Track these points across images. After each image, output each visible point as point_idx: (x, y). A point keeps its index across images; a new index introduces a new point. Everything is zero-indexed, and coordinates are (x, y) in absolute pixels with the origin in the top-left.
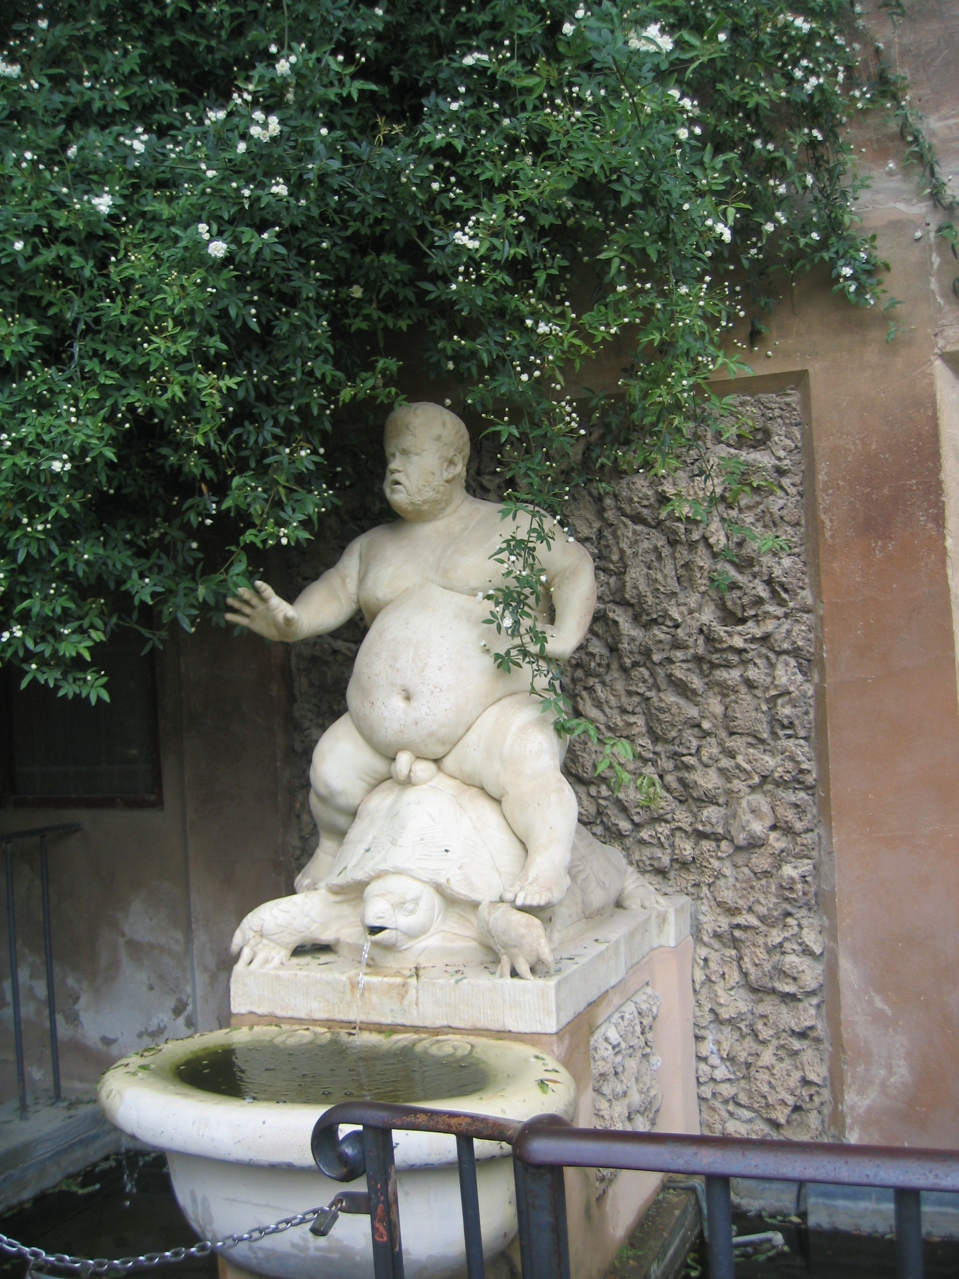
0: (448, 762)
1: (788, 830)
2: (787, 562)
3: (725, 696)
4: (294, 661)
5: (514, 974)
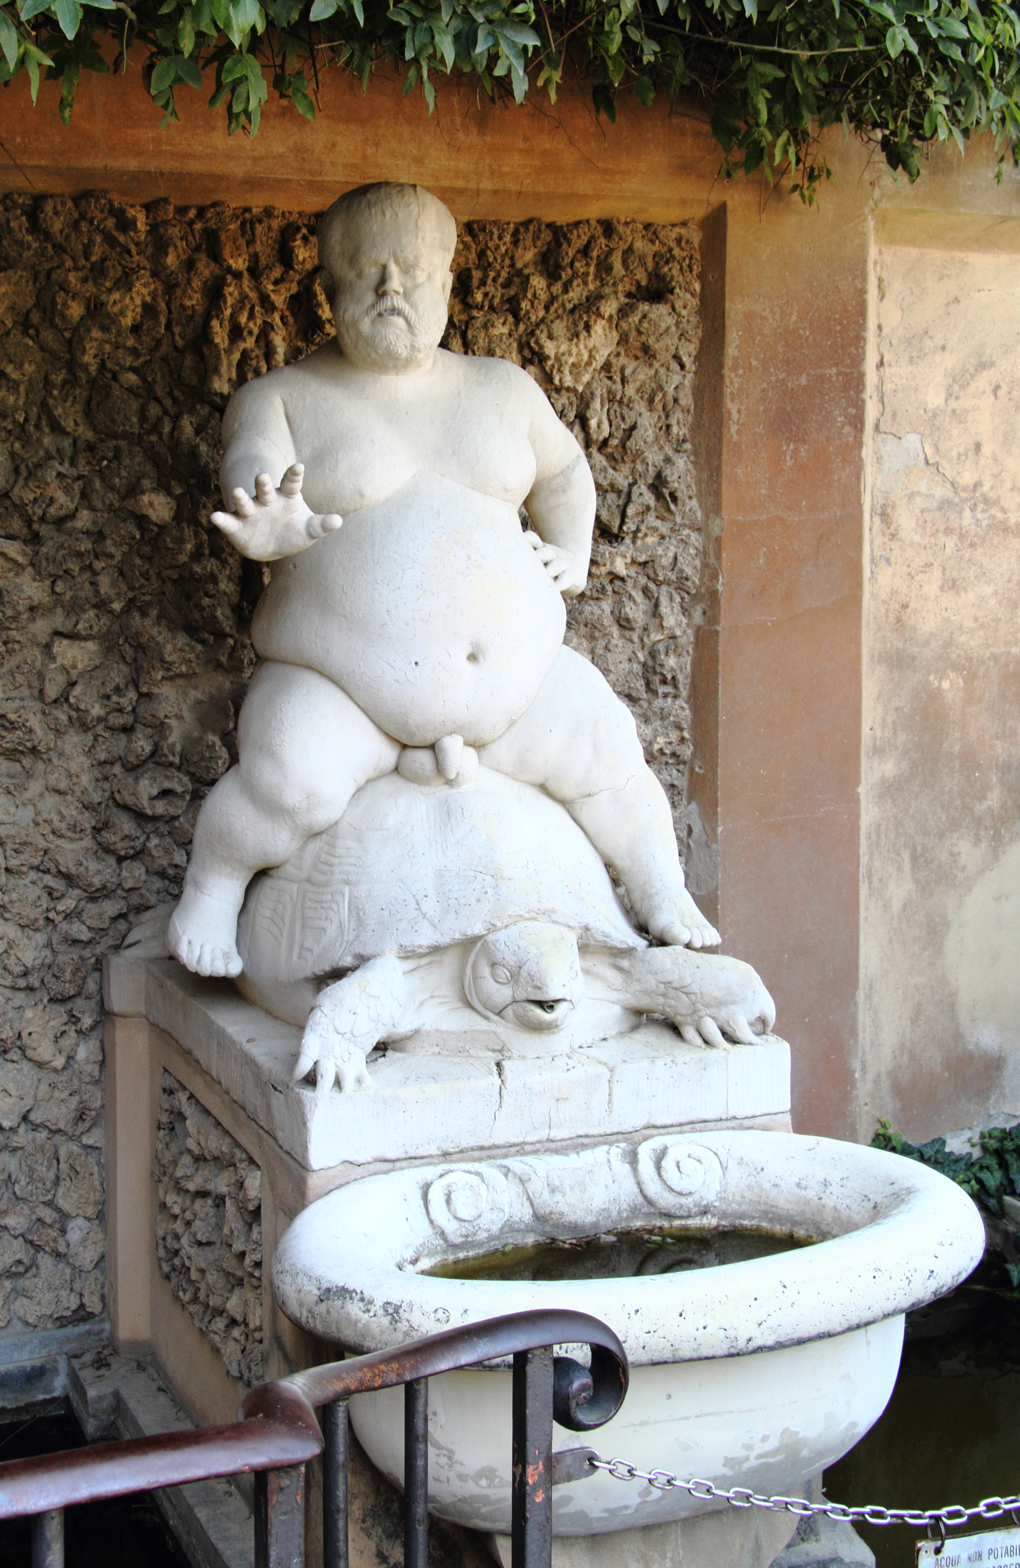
0: (500, 751)
3: (592, 638)
5: (731, 1039)
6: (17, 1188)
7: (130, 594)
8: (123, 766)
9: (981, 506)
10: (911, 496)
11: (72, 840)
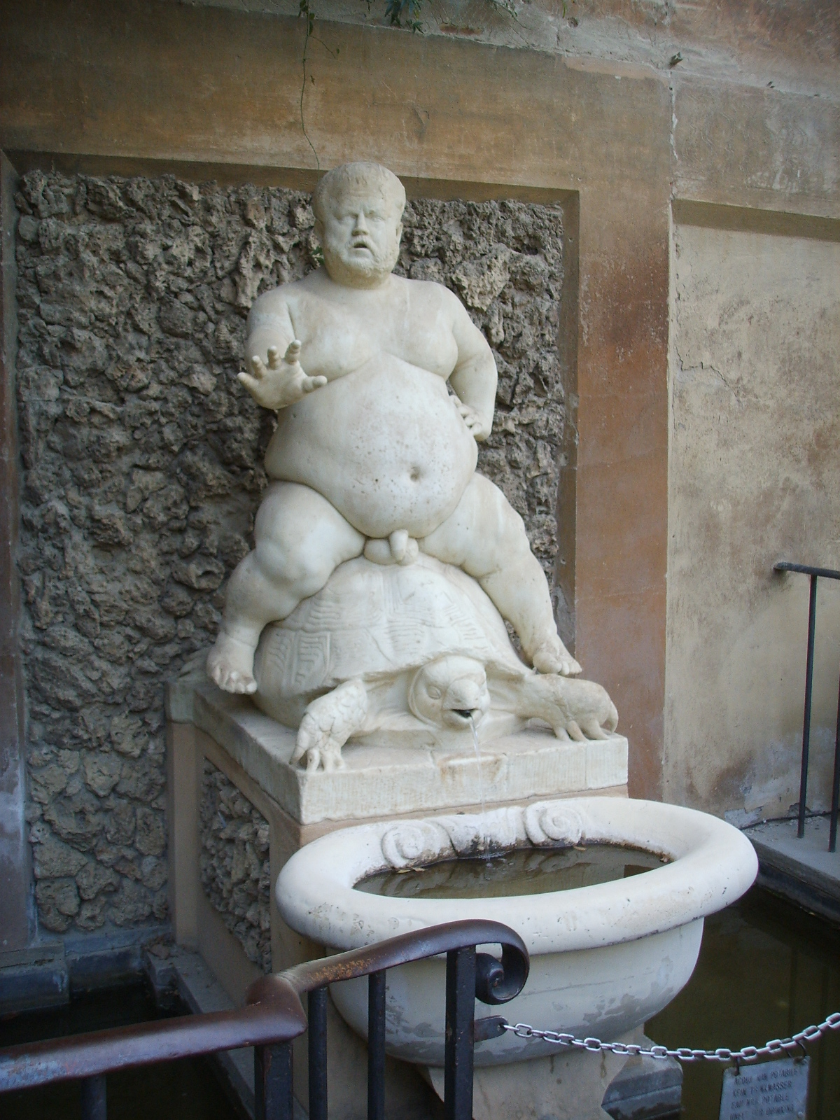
2: (550, 358)
4: (32, 422)
6: (108, 836)
7: (185, 441)
8: (179, 555)
9: (742, 393)
10: (698, 385)
11: (144, 604)
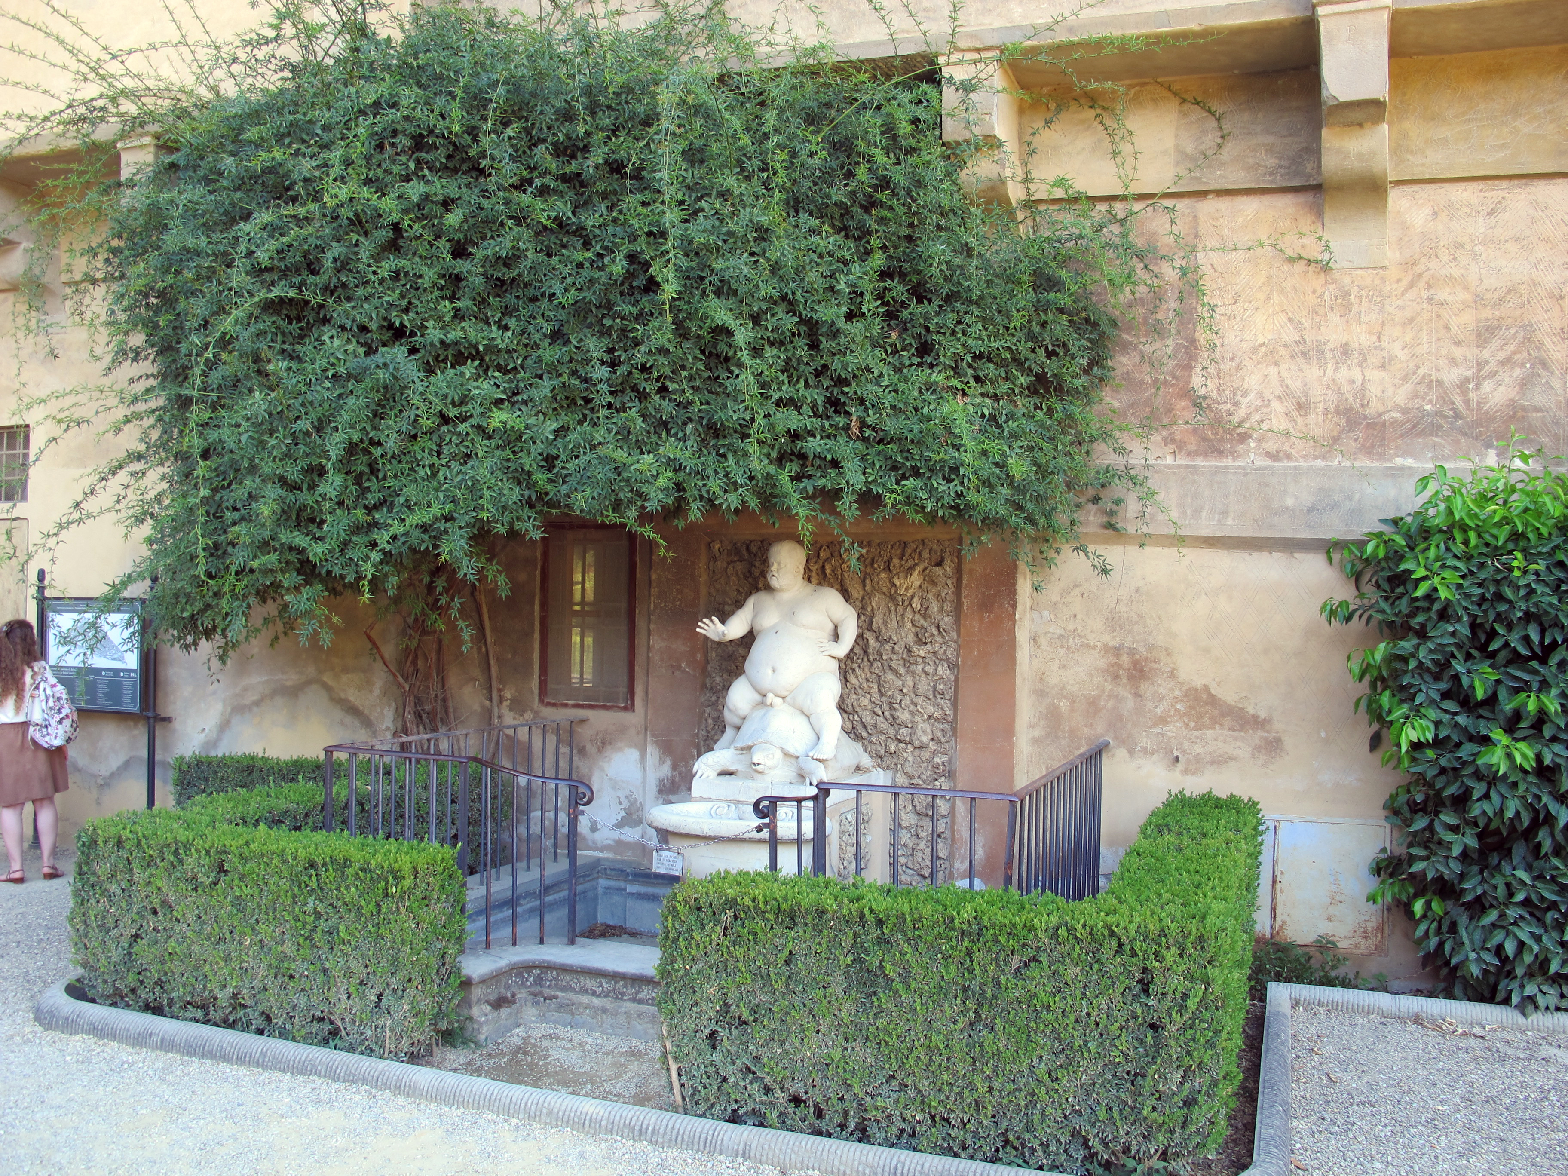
1: (939, 742)
2: (946, 619)
